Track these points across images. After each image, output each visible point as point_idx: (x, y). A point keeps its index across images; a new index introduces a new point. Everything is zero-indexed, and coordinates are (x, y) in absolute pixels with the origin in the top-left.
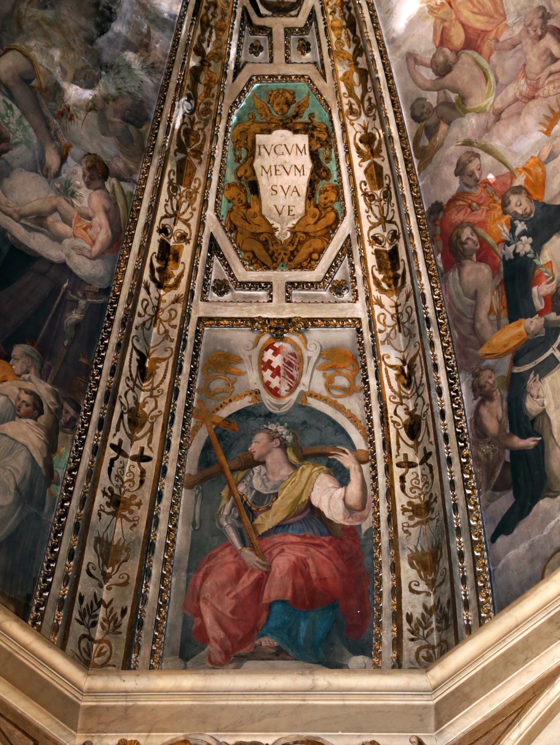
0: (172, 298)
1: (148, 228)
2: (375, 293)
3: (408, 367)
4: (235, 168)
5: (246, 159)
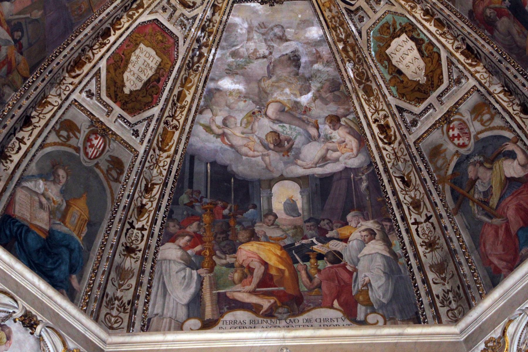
1: (369, 125)
2: (472, 69)
3: (507, 87)
5: (389, 65)
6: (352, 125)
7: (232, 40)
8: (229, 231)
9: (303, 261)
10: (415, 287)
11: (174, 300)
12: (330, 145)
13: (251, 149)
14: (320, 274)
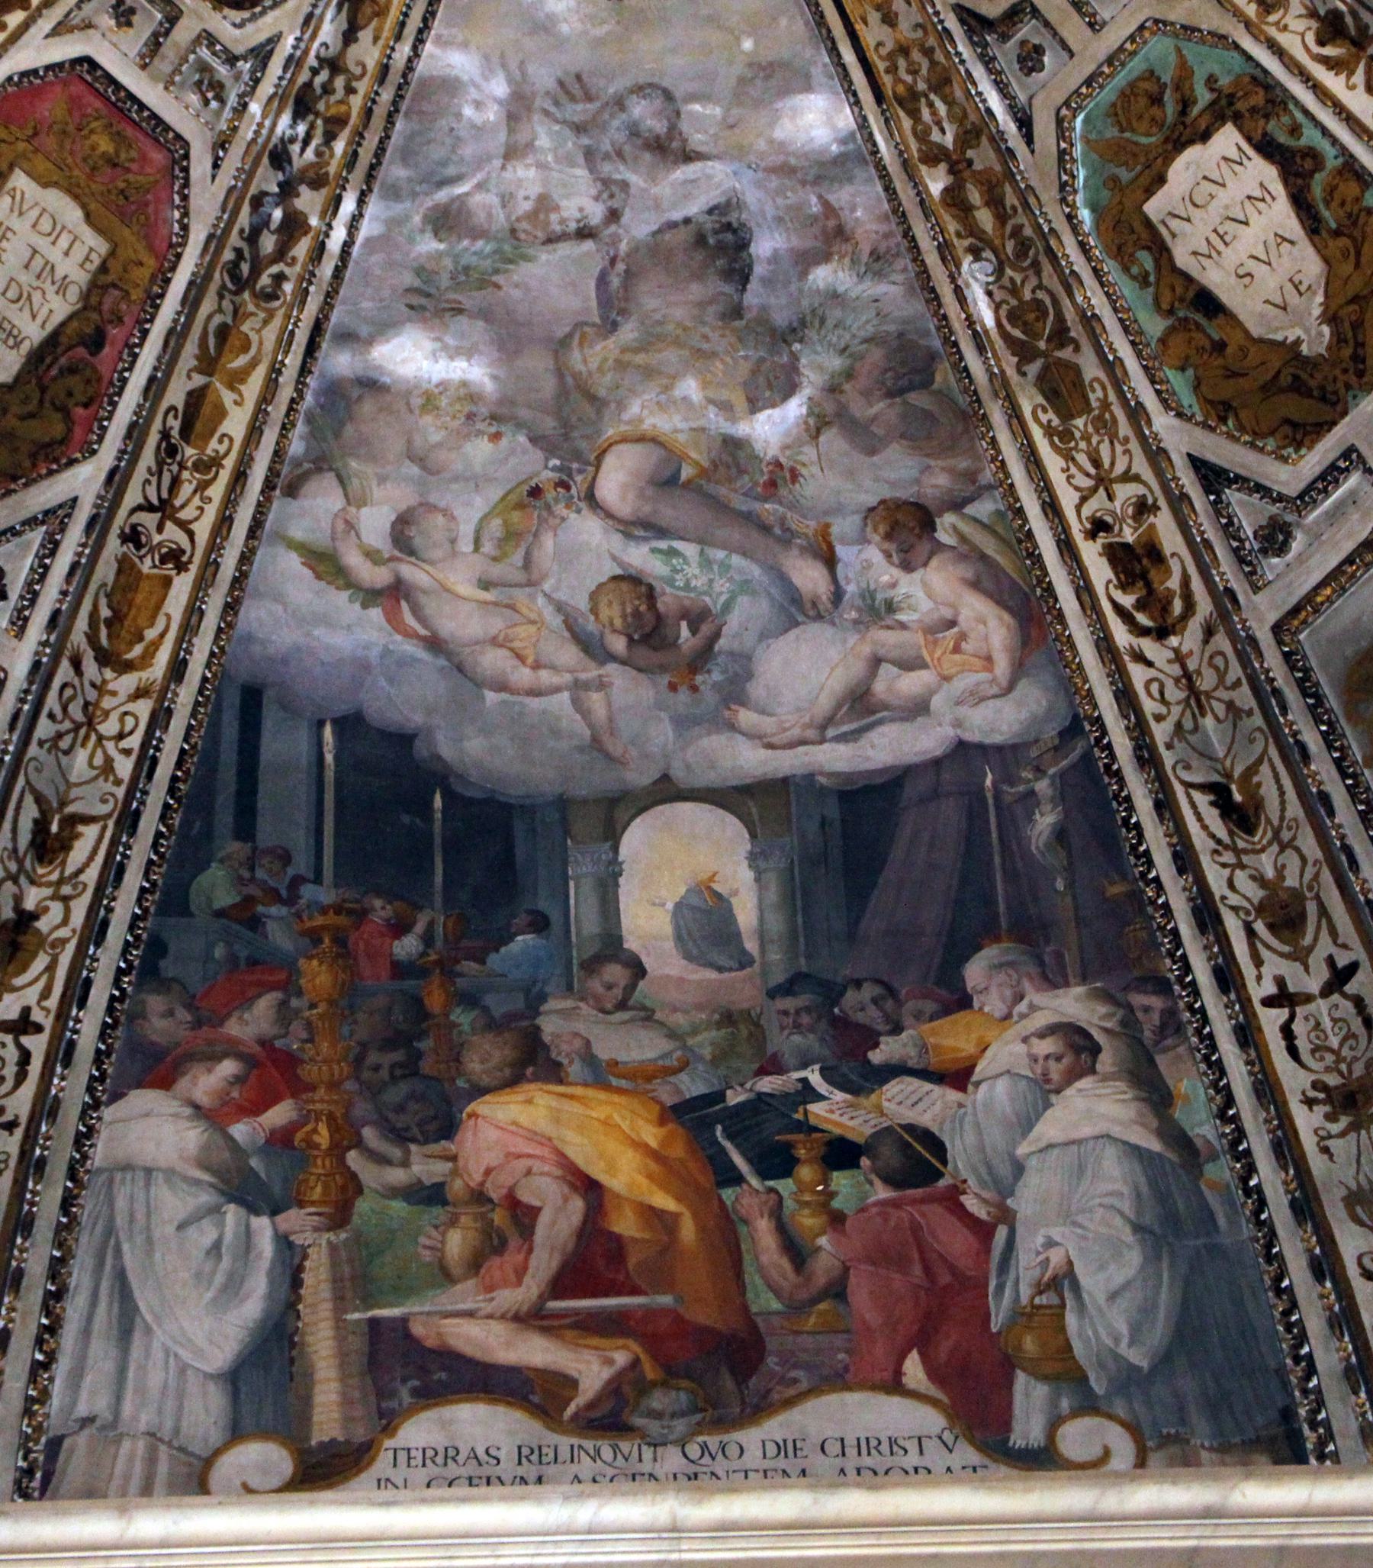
0: (1199, 635)
1: (1067, 548)
4: (1150, 300)
5: (1158, 267)
6: (990, 547)
7: (437, 153)
8: (422, 1035)
9: (764, 1175)
10: (1279, 1292)
11: (167, 1352)
12: (887, 639)
13: (520, 658)
14: (843, 1232)
